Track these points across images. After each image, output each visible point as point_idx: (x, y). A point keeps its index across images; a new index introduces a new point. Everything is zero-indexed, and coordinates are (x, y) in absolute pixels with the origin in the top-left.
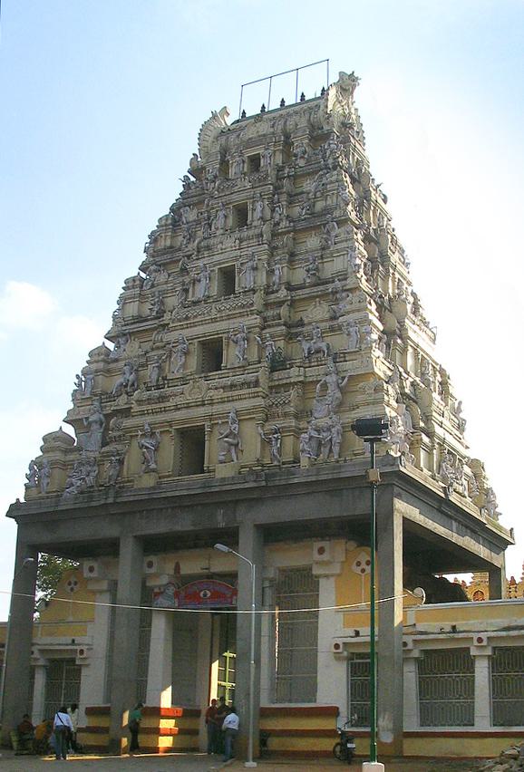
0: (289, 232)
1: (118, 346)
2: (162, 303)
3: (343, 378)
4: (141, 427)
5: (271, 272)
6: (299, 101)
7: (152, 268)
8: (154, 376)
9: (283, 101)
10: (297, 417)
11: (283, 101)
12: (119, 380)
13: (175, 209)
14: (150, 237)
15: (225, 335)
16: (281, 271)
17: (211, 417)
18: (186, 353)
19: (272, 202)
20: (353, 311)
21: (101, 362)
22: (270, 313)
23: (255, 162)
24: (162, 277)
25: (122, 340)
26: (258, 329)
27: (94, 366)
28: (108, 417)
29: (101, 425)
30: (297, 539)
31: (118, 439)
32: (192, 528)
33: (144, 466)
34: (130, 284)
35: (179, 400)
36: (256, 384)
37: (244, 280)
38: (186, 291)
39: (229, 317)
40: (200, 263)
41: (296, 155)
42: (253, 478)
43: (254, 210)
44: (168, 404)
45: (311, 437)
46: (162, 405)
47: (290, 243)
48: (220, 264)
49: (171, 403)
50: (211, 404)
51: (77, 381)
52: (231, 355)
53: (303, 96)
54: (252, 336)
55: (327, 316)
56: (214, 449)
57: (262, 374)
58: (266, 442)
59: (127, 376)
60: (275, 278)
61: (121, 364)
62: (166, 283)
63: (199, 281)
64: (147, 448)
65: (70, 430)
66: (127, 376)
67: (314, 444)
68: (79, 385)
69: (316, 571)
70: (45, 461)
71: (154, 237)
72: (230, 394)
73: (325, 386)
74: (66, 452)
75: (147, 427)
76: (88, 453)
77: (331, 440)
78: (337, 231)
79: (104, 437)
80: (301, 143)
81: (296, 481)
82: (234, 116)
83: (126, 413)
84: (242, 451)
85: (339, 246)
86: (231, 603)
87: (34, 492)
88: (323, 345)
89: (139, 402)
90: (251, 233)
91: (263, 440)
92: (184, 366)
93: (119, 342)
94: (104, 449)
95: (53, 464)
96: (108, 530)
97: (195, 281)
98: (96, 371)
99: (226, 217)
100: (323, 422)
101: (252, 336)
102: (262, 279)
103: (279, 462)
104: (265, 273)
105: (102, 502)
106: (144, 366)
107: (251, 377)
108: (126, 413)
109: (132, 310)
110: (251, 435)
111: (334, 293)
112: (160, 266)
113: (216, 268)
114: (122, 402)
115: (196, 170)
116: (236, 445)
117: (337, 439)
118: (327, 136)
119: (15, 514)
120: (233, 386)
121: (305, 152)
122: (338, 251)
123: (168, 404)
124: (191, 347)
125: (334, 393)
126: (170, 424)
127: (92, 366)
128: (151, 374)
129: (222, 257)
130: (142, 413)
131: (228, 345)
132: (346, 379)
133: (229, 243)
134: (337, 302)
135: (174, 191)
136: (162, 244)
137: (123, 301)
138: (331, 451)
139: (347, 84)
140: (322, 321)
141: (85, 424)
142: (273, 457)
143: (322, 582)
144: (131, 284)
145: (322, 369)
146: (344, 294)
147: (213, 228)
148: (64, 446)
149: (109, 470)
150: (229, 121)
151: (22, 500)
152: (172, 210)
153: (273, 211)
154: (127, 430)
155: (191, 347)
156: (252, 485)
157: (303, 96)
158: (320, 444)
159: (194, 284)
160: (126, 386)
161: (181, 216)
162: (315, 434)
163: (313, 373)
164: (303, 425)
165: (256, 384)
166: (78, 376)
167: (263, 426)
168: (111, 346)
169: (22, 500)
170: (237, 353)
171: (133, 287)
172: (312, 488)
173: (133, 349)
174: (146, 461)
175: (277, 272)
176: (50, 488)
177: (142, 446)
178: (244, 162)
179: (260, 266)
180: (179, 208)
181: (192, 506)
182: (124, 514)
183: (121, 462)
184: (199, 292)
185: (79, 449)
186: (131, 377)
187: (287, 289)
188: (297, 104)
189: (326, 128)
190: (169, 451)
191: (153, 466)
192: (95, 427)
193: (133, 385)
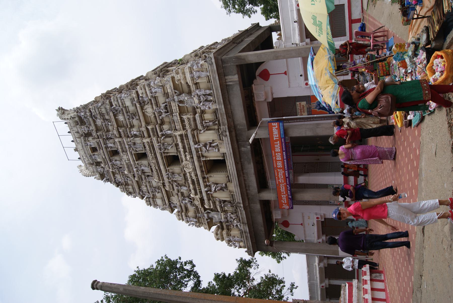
0: (118, 129)
1: (176, 207)
2: (155, 188)
3: (176, 93)
4: (207, 192)
5: (136, 136)
6: (70, 134)
7: (141, 193)
8: (185, 188)
9: (72, 141)
10: (195, 113)
11: (72, 141)
12: (189, 205)
13: (118, 184)
14: (129, 195)
15: (163, 155)
16: (134, 131)
17: (199, 157)
18: (173, 173)
19: (108, 139)
20: (146, 92)
21: (183, 214)
22: (151, 134)
23: (94, 150)
24: (144, 189)
25: (172, 205)
26: (159, 139)
27: (184, 217)
28: (205, 209)
29: (209, 213)
30: (254, 110)
31: (214, 203)
32: (252, 164)
33: (225, 190)
34: (149, 203)
35: (193, 175)
36: (181, 136)
37: (140, 150)
38: (148, 176)
39: (155, 154)
40: (135, 170)
41: (88, 131)
42: (224, 134)
43: (111, 147)
44: (195, 180)
45: (203, 105)
46: (196, 182)
47: (123, 128)
48: (134, 161)
49: (194, 178)
50: (193, 158)
51: (191, 226)
52: (172, 151)
53: (69, 132)
54: (162, 142)
55: (150, 106)
56: (213, 155)
57: (177, 133)
58: (208, 128)
59: (187, 201)
60: (138, 133)
61: (182, 204)
62: (146, 186)
63: (143, 170)
64: (215, 189)
65: (214, 228)
66: (187, 201)
67: (207, 103)
68: (193, 224)
69: (270, 100)
70: (227, 239)
71: (129, 193)
72: (187, 149)
73: (181, 102)
74: (223, 229)
75: (206, 189)
76: (223, 218)
77: (204, 95)
78: (114, 106)
79: (212, 210)
80: (84, 129)
81: (224, 110)
82: (80, 163)
83: (202, 200)
84: (213, 140)
85: (120, 104)
86: (289, 143)
87: (242, 244)
88: (162, 106)
89: (196, 194)
90: (119, 147)
91: (207, 130)
92: (179, 174)
93: (174, 207)
94: (219, 210)
95: (228, 235)
96: (258, 207)
97: (143, 172)
98: (186, 216)
99: (116, 161)
100: (196, 101)
101: (162, 142)
102: (138, 140)
103: (216, 121)
104: (136, 139)
105: (243, 209)
106: (182, 194)
107: (179, 138)
108: (202, 200)
109: (159, 201)
110: (206, 136)
111: (140, 104)
112: (140, 190)
113: (136, 162)
114: (198, 203)
115: (102, 176)
116: (211, 143)
117: (203, 92)
118: (80, 117)
119: (252, 252)
120: (184, 148)
121: (87, 127)
122: (123, 104)
123: (195, 180)
124: (171, 171)
125: (184, 97)
126: (204, 178)
127: (184, 219)
128: (184, 189)
129: (131, 160)
130: (201, 192)
131: (167, 153)
132: (176, 91)
133: (125, 157)
134: (144, 102)
135: (110, 186)
136: (131, 190)
137: (156, 205)
138: (209, 95)
139: (62, 111)
140: (153, 108)
141: (209, 220)
142: (214, 124)
143: (275, 97)
144: (149, 203)
145: (173, 104)
146: (140, 99)
147: (121, 166)
148: (220, 230)
149: (228, 208)
150: (83, 165)
151: (246, 249)
152: (118, 186)
153: (111, 138)
154: (209, 200)
155: (171, 171)
156: (228, 133)
157: (69, 132)
158: (206, 100)
159: (144, 173)
160: (192, 202)
161: (120, 182)
162: (201, 104)
163: (175, 107)
164: (198, 110)
165: (181, 136)
166: (189, 225)
167: (201, 131)
168: (176, 210)
169: (246, 249)
170: (170, 148)
171: (150, 201)
172: (227, 101)
173: (175, 200)
174: (222, 189)
175: (135, 133)
176: (239, 236)
177: (215, 191)
178: (94, 155)
179: (133, 142)
180: (117, 183)
181: (241, 163)
182: (248, 199)
183: (225, 201)
184: (147, 170)
185: (221, 222)
186: (187, 199)
187: (141, 127)
188: (72, 135)
189: (77, 119)
190: (217, 177)
191: (224, 185)
192: (210, 215)
193: (191, 199)
